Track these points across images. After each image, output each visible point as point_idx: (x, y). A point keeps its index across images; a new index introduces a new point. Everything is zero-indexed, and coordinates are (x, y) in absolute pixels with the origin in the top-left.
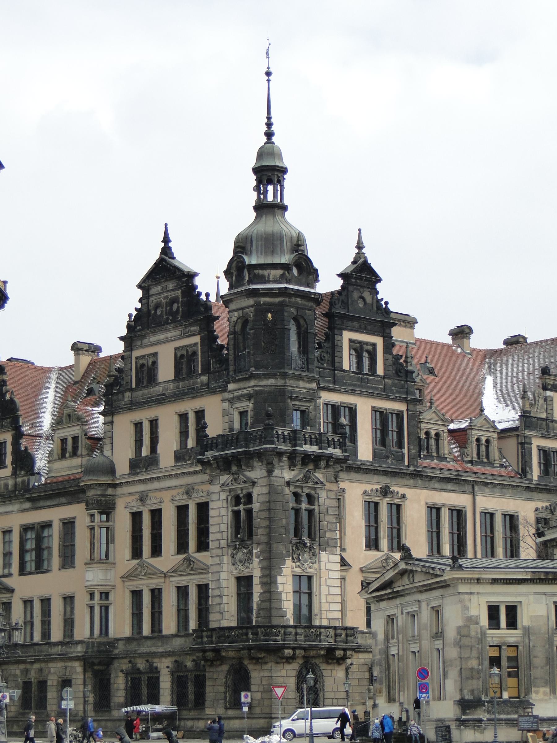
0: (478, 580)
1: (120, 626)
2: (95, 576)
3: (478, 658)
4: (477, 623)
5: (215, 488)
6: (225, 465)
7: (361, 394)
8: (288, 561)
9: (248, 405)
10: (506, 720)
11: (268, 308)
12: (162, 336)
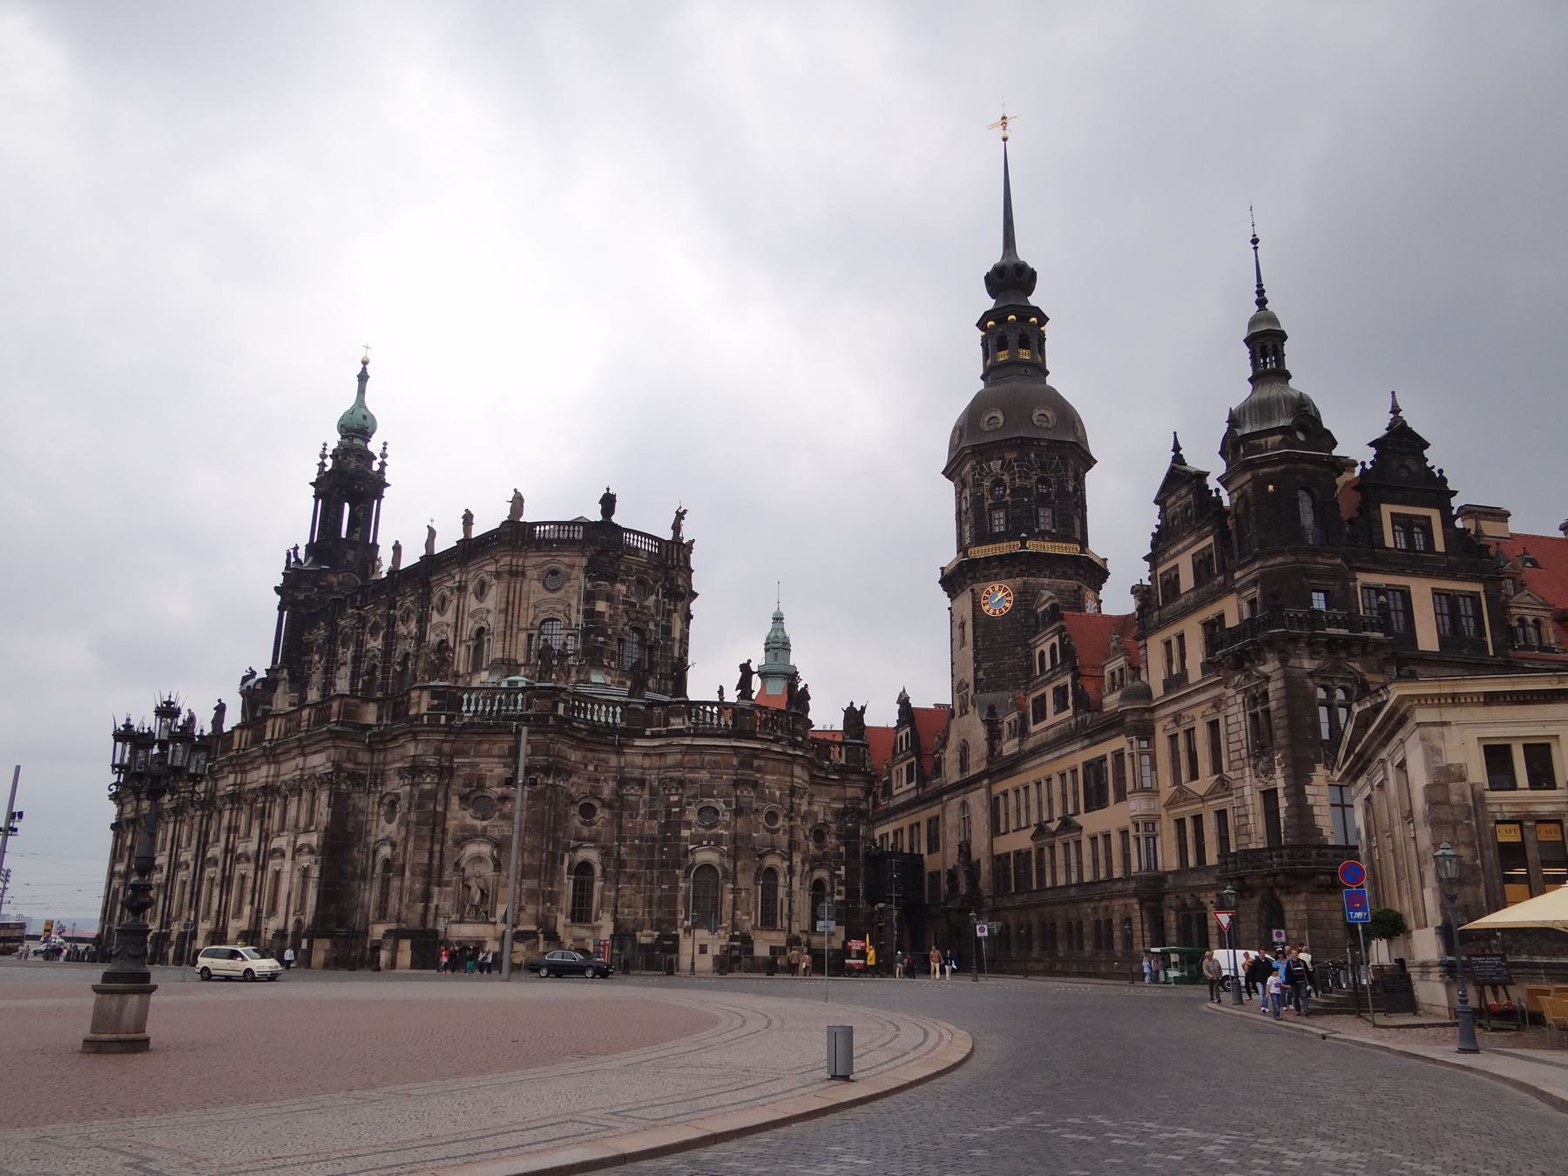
0: (1454, 696)
1: (1168, 860)
3: (1471, 844)
4: (1463, 779)
5: (1231, 692)
6: (1241, 661)
7: (1414, 574)
8: (1320, 768)
9: (1255, 592)
10: (1546, 966)
11: (1269, 479)
12: (1180, 547)
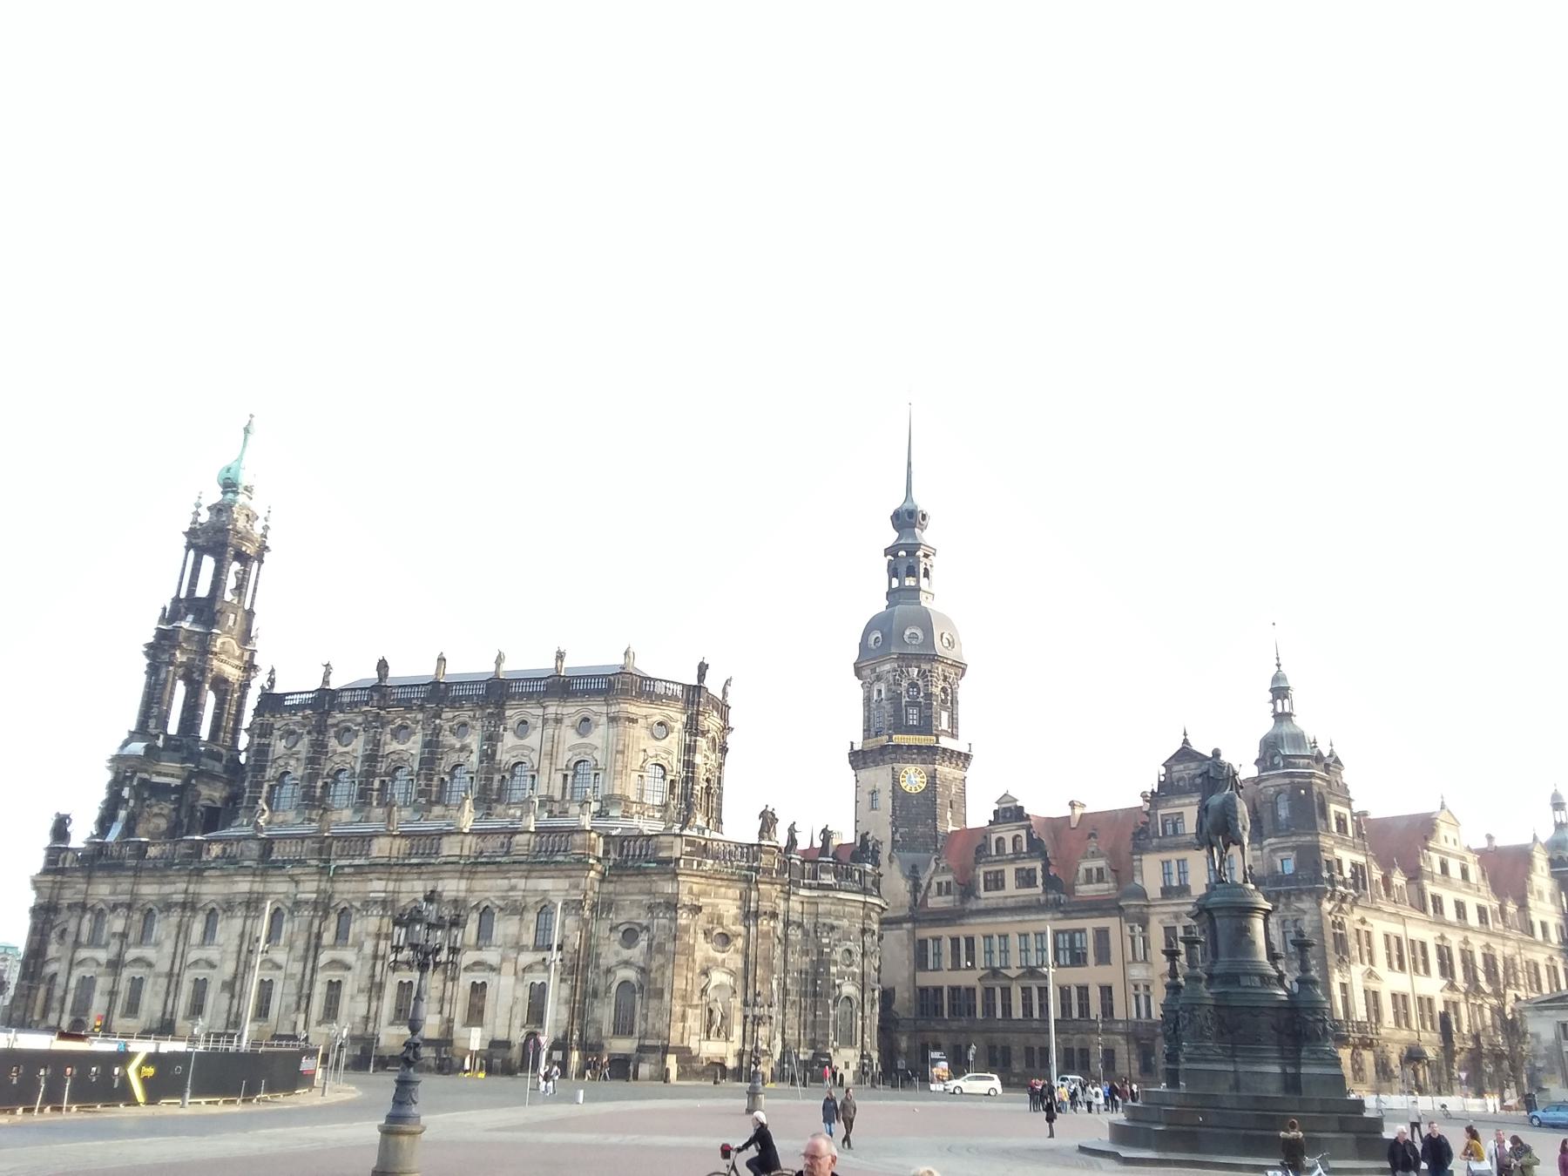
2: (1138, 972)
9: (1293, 855)
